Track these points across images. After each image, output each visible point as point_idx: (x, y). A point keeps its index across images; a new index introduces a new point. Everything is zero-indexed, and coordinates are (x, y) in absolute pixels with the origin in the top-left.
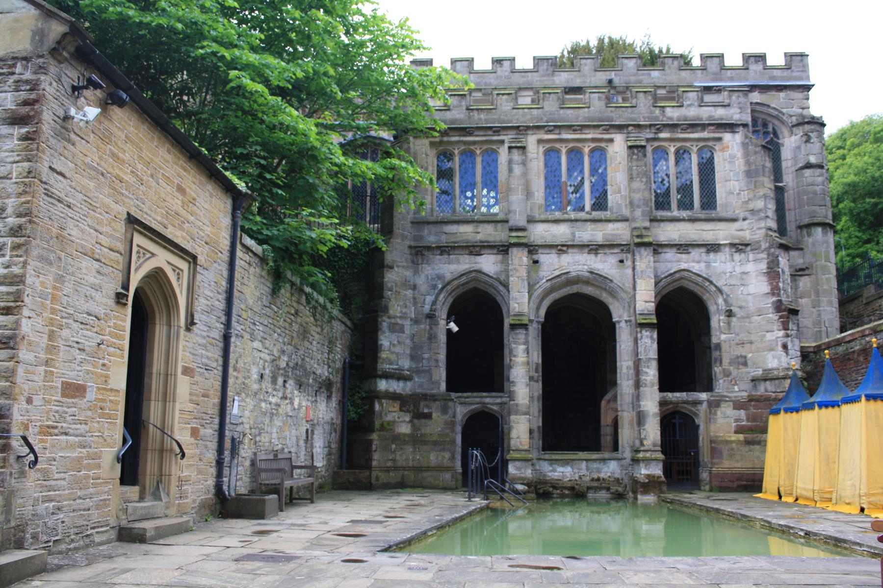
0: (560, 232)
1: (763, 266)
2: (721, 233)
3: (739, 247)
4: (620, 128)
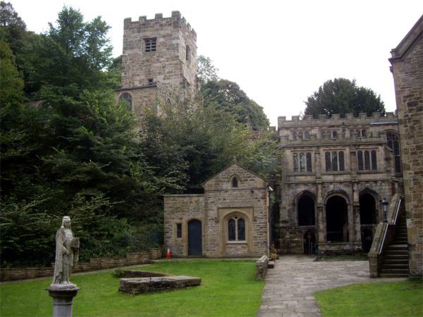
0: (330, 178)
1: (391, 187)
2: (378, 177)
3: (383, 181)
4: (349, 146)
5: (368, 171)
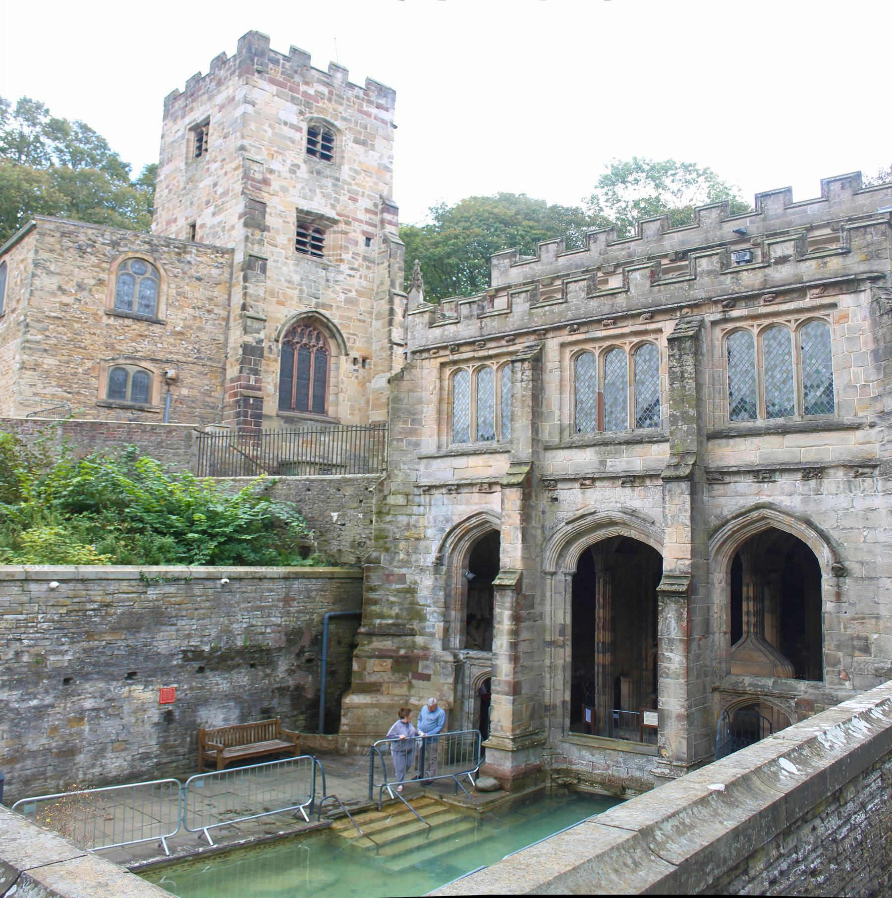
5: (780, 421)
